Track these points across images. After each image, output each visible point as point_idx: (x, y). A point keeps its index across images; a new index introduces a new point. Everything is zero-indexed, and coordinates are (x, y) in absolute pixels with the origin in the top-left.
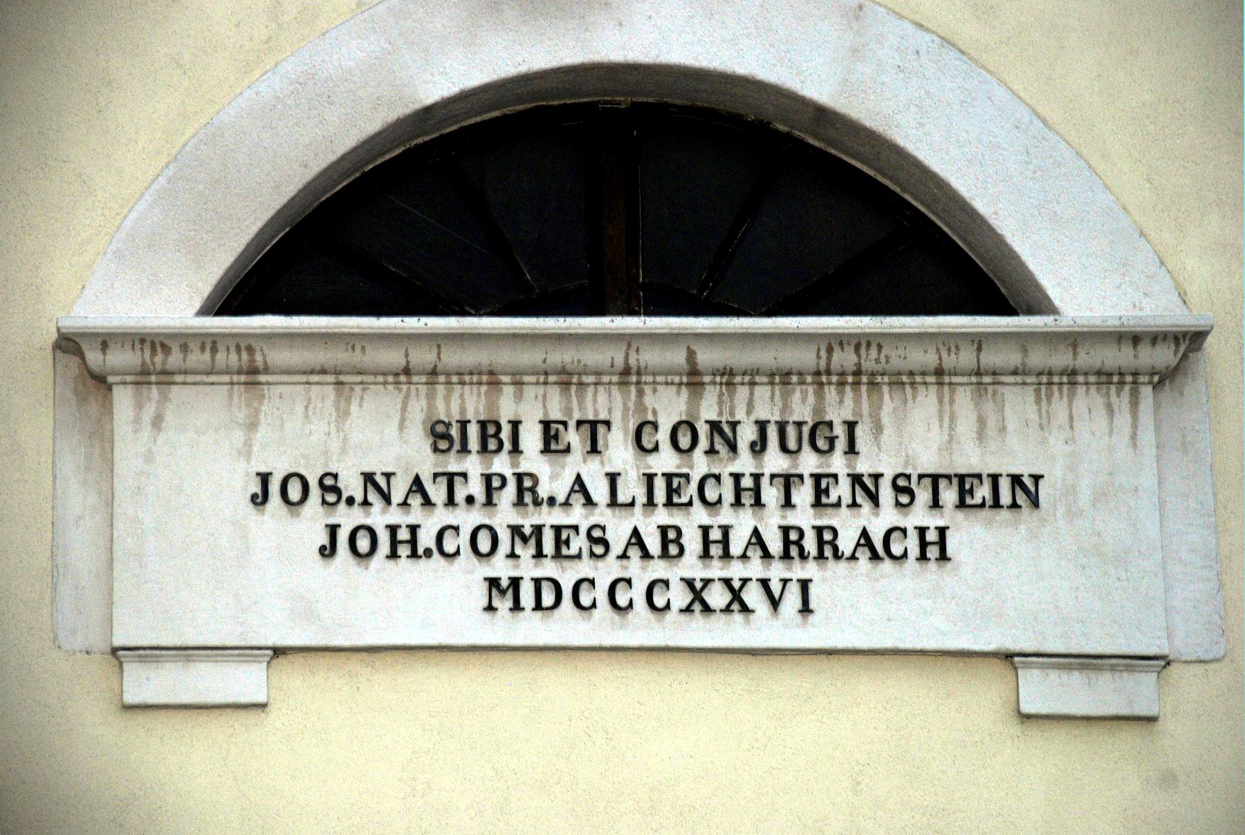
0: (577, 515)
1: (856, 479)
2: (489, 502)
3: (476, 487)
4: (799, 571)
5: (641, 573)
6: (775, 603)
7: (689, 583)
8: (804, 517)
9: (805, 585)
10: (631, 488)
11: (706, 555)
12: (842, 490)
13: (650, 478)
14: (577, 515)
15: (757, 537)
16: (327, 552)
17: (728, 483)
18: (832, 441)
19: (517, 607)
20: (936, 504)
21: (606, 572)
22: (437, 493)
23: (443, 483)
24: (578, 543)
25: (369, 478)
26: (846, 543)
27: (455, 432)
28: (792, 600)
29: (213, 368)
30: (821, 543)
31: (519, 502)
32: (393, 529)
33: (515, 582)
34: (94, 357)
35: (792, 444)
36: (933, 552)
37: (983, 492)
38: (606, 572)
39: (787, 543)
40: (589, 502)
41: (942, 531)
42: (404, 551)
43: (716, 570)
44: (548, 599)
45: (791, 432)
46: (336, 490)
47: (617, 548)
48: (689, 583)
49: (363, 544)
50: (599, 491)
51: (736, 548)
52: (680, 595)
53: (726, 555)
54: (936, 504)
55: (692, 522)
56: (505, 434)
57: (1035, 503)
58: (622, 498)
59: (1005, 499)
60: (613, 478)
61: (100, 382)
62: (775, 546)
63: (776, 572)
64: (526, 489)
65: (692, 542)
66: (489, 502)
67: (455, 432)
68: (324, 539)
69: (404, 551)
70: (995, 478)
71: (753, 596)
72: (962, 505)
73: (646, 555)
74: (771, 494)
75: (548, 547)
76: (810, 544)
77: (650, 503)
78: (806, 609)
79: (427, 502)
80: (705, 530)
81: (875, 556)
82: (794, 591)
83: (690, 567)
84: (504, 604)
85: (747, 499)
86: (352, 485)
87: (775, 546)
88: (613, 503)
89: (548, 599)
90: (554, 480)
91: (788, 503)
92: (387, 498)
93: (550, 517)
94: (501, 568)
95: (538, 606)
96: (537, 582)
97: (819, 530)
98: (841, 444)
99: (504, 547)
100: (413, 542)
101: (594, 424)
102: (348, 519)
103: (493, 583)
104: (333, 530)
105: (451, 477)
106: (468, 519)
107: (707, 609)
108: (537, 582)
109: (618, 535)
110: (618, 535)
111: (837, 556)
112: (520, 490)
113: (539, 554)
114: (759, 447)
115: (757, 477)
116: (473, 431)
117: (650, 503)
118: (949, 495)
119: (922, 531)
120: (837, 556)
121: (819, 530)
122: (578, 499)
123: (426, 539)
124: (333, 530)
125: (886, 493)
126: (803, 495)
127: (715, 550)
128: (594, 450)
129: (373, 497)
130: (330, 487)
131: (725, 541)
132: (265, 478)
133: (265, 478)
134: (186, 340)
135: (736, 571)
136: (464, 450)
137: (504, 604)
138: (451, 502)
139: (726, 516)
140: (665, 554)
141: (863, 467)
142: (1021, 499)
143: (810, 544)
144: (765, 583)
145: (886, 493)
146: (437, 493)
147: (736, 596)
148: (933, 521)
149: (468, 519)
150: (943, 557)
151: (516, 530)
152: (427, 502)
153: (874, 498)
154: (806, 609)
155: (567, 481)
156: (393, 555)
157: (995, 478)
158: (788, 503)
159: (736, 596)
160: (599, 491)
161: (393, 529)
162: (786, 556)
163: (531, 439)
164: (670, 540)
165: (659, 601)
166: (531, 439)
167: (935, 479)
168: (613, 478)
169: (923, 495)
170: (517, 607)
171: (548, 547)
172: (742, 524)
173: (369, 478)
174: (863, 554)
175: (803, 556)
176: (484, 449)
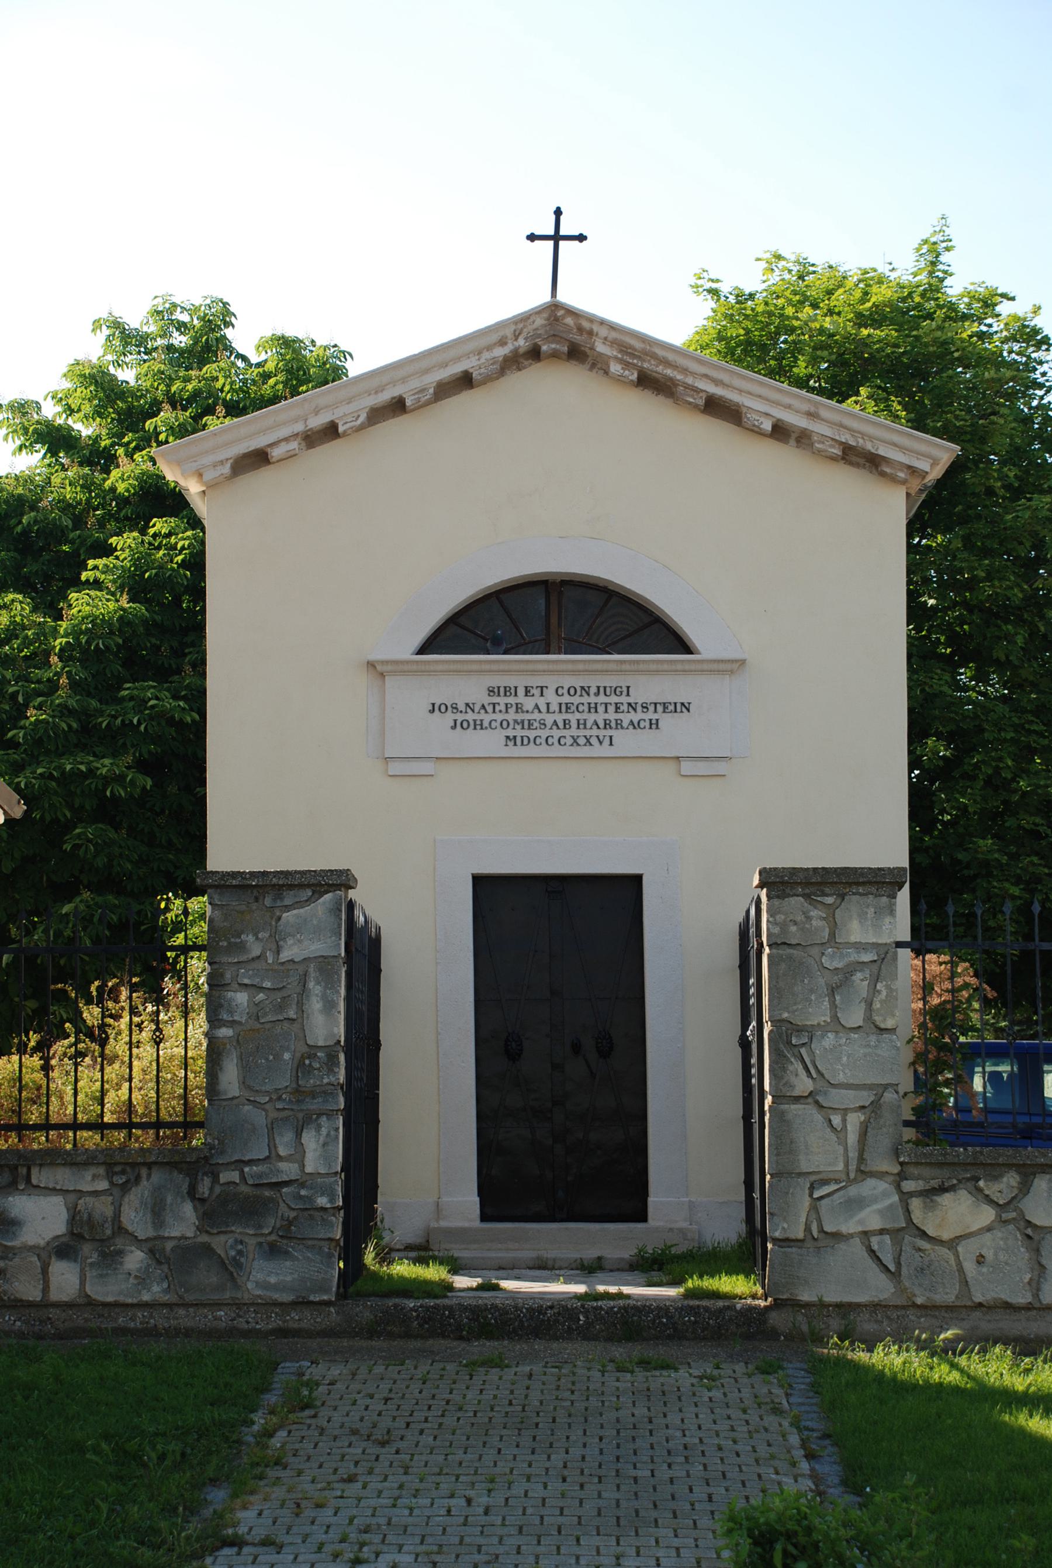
0: (536, 716)
1: (629, 704)
2: (507, 712)
3: (503, 708)
4: (609, 732)
5: (557, 733)
6: (601, 743)
7: (572, 737)
8: (612, 716)
9: (611, 737)
10: (554, 707)
11: (578, 728)
12: (625, 707)
13: (560, 704)
14: (536, 716)
15: (596, 723)
16: (454, 727)
17: (586, 706)
18: (621, 692)
19: (515, 744)
20: (656, 711)
21: (544, 734)
22: (490, 709)
23: (491, 706)
24: (536, 724)
25: (467, 705)
26: (625, 724)
27: (496, 690)
28: (607, 741)
29: (498, 598)
30: (617, 724)
31: (517, 712)
32: (475, 721)
33: (515, 737)
34: (379, 668)
35: (608, 693)
36: (654, 726)
37: (671, 708)
38: (544, 734)
39: (605, 724)
40: (540, 711)
41: (657, 720)
42: (478, 727)
43: (582, 732)
44: (526, 741)
45: (608, 690)
46: (456, 708)
47: (549, 726)
48: (572, 737)
49: (465, 725)
50: (543, 708)
51: (589, 725)
52: (570, 741)
53: (585, 728)
54: (656, 711)
55: (573, 718)
56: (513, 691)
57: (688, 710)
58: (551, 710)
59: (679, 709)
60: (548, 704)
61: (382, 675)
62: (602, 725)
63: (602, 733)
64: (518, 708)
65: (574, 724)
66: (507, 712)
67: (496, 690)
68: (452, 724)
69: (478, 727)
70: (675, 704)
71: (594, 741)
72: (664, 712)
73: (558, 728)
74: (601, 709)
75: (526, 726)
76: (613, 724)
77: (560, 711)
78: (611, 744)
79: (486, 712)
80: (578, 720)
81: (635, 728)
82: (607, 740)
83: (574, 732)
84: (511, 744)
85: (593, 710)
86: (461, 707)
87: (602, 725)
88: (548, 711)
89: (526, 741)
90: (529, 703)
91: (606, 711)
92: (473, 711)
93: (527, 717)
94: (511, 733)
95: (522, 744)
96: (522, 737)
97: (616, 720)
98: (625, 693)
99: (511, 726)
100: (481, 725)
101: (542, 688)
102: (460, 717)
103: (508, 737)
104: (455, 721)
105: (494, 705)
106: (499, 717)
107: (578, 745)
108: (522, 737)
109: (549, 723)
110: (549, 723)
111: (622, 728)
112: (517, 708)
113: (523, 728)
114: (597, 694)
115: (596, 704)
116: (502, 690)
117: (560, 711)
118: (660, 708)
119: (651, 720)
120: (622, 728)
121: (616, 720)
122: (536, 711)
123: (486, 724)
124: (455, 721)
125: (639, 708)
126: (611, 709)
127: (581, 726)
128: (542, 695)
129: (469, 710)
130: (455, 708)
131: (585, 724)
132: (433, 705)
133: (433, 705)
134: (408, 662)
135: (588, 733)
136: (499, 695)
137: (511, 744)
138: (494, 712)
139: (585, 716)
140: (565, 728)
141: (631, 700)
142: (684, 709)
143: (613, 724)
144: (598, 737)
145: (639, 708)
146: (490, 709)
147: (588, 741)
148: (655, 717)
149: (499, 717)
150: (657, 728)
151: (516, 721)
152: (486, 712)
153: (635, 710)
154: (611, 744)
155: (532, 705)
156: (475, 728)
157: (675, 704)
158: (606, 711)
159: (588, 741)
160: (543, 708)
161: (475, 721)
162: (605, 728)
163: (521, 692)
164: (566, 724)
165: (562, 742)
166: (521, 692)
167: (656, 704)
168: (548, 704)
169: (652, 708)
170: (515, 744)
171: (526, 726)
172: (591, 718)
173: (467, 705)
174: (631, 727)
175: (611, 728)
176: (505, 695)
